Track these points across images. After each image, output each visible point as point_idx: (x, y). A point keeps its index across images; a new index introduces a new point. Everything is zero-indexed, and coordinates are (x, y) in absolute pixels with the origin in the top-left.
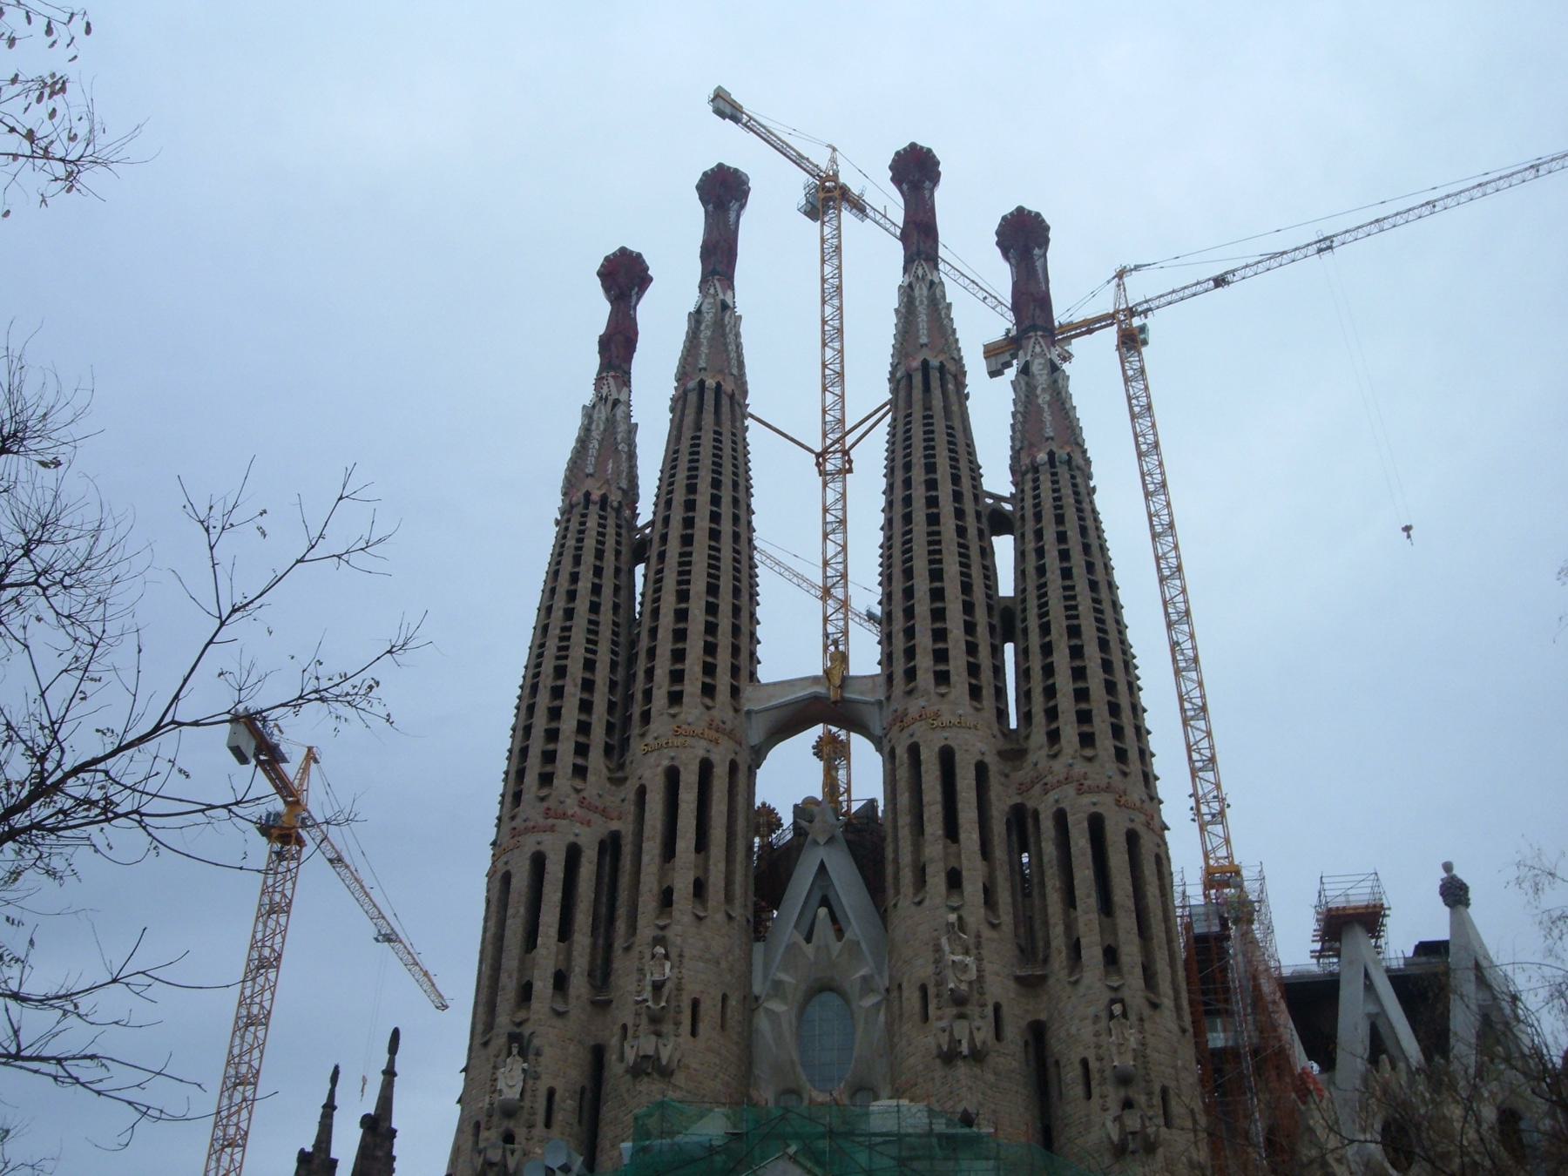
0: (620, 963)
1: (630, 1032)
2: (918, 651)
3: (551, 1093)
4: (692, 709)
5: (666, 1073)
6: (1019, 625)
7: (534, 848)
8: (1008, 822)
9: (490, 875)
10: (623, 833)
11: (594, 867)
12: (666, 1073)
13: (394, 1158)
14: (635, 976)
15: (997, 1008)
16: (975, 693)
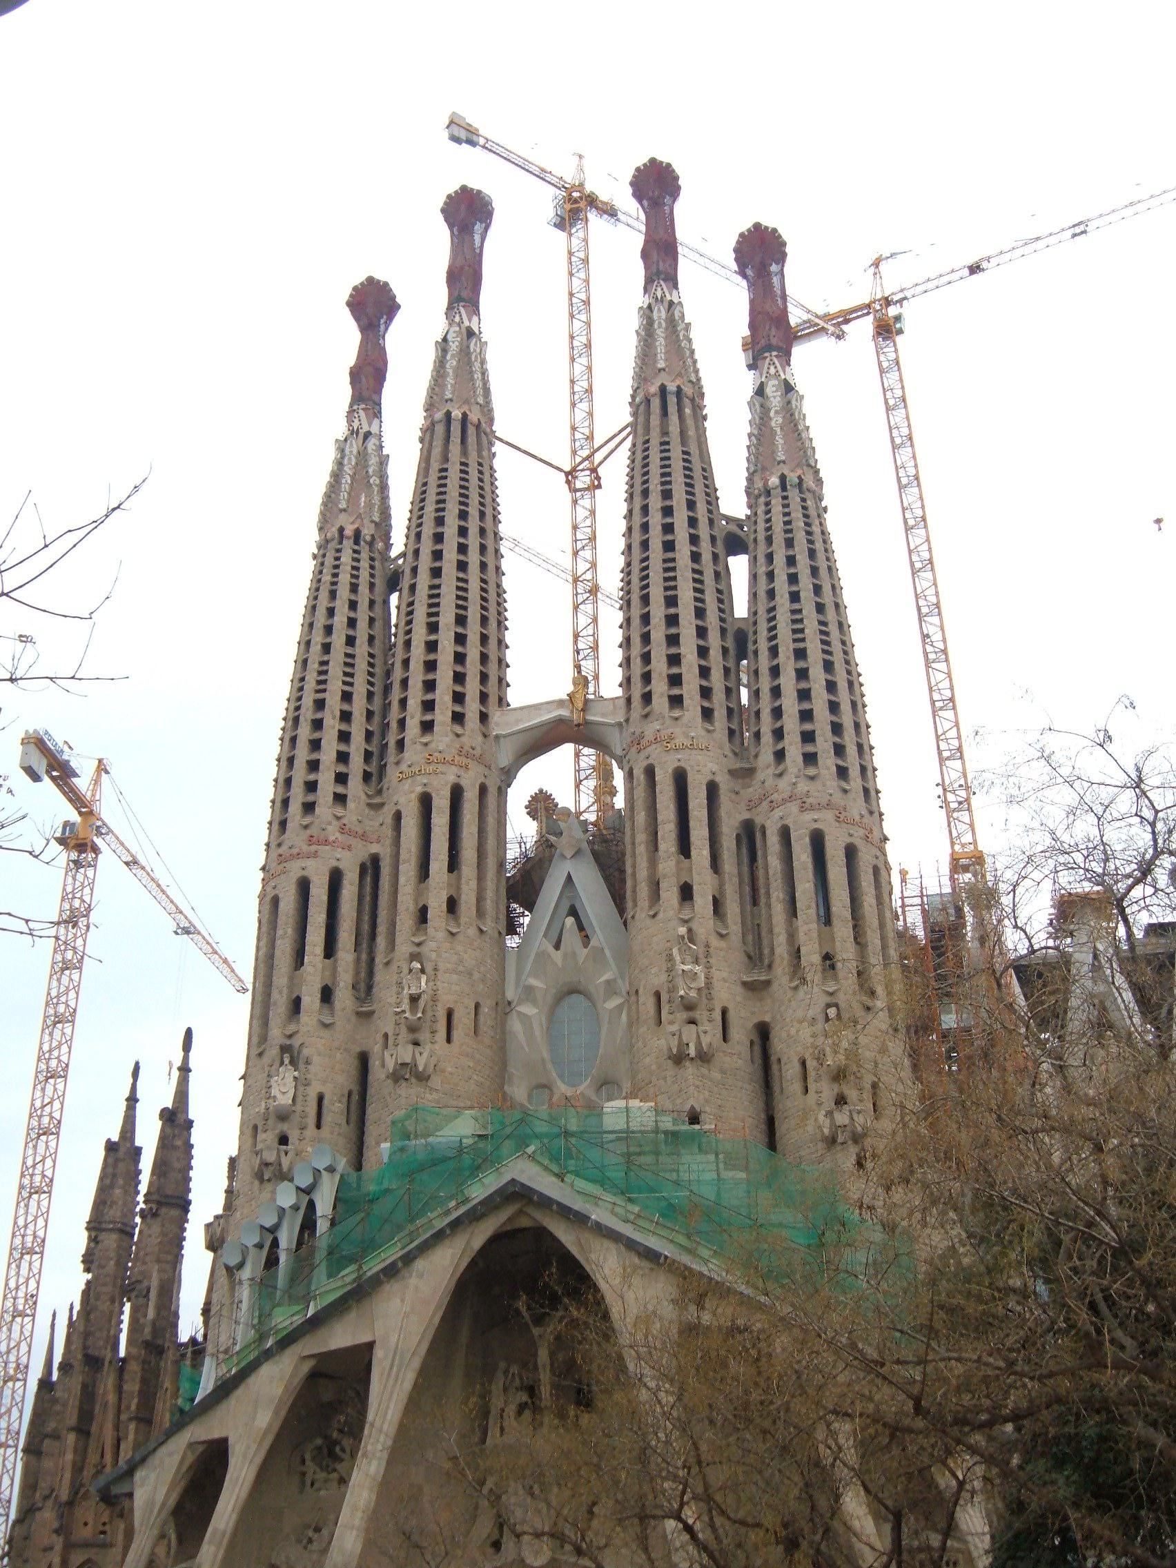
0: (380, 976)
1: (390, 1042)
2: (653, 675)
3: (320, 1099)
4: (443, 736)
5: (422, 1078)
6: (751, 647)
7: (301, 873)
8: (738, 835)
9: (262, 897)
10: (382, 855)
11: (355, 889)
12: (422, 1078)
13: (192, 1146)
14: (394, 989)
15: (724, 1012)
16: (707, 714)
